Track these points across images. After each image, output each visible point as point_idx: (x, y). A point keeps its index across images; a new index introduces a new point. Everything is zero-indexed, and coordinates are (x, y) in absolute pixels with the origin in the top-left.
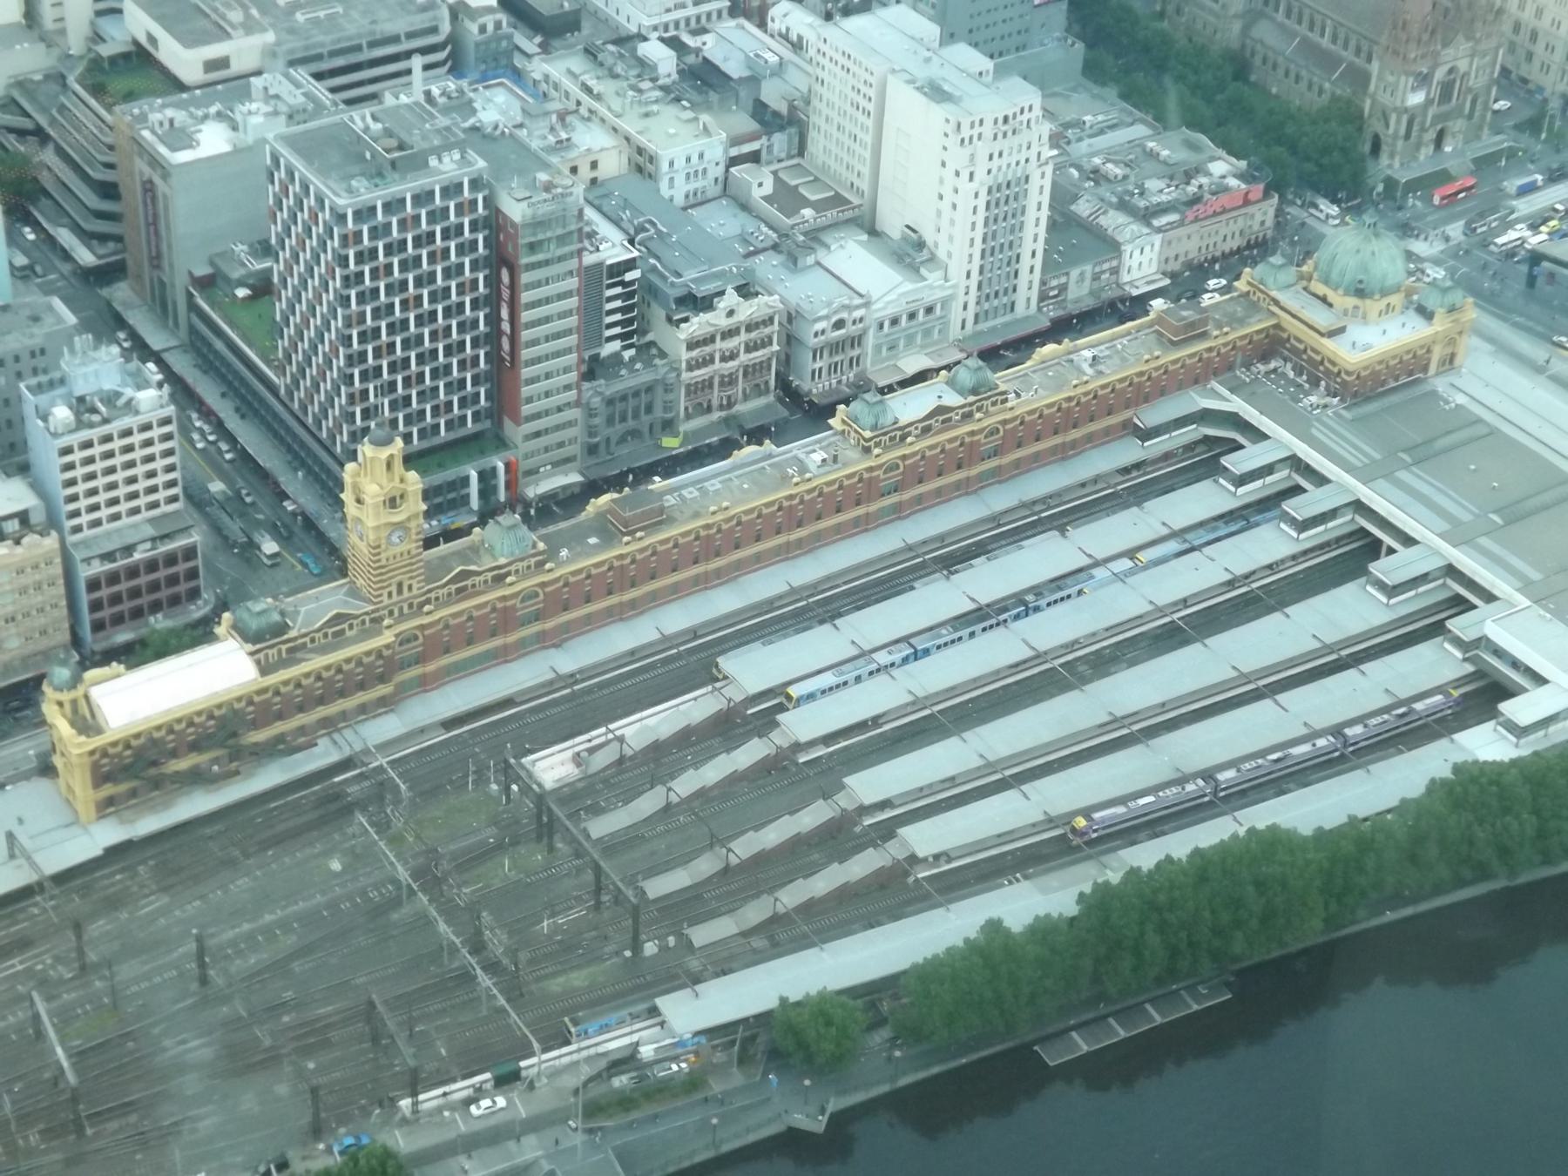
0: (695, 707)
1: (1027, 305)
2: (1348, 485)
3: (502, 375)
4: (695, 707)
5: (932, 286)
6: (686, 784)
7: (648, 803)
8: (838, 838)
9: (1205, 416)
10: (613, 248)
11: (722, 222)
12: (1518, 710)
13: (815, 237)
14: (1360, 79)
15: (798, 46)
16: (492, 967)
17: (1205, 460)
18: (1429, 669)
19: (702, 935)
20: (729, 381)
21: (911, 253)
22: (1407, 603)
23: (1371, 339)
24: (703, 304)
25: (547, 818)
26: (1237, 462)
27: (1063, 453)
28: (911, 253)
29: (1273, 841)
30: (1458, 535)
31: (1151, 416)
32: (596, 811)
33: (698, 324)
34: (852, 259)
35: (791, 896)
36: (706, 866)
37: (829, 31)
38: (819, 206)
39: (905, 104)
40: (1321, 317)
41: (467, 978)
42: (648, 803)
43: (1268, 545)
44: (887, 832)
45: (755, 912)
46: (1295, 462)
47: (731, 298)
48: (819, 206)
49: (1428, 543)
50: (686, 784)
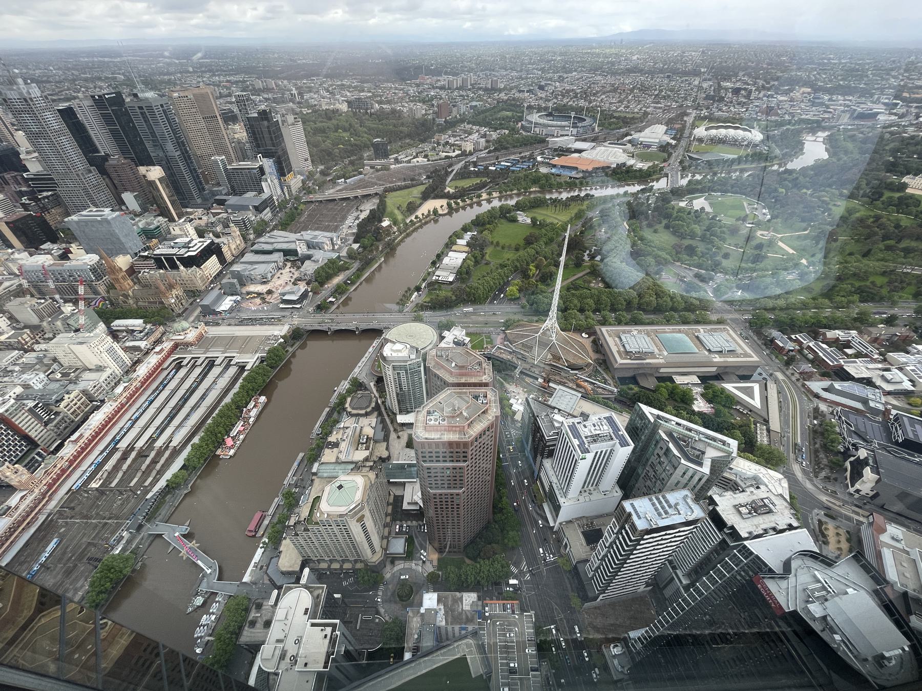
0: (117, 456)
1: (129, 362)
2: (203, 356)
3: (26, 438)
4: (117, 456)
5: (108, 372)
6: (125, 467)
7: (120, 475)
8: (160, 453)
9: (174, 360)
10: (31, 404)
11: (54, 386)
12: (248, 367)
13: (77, 378)
14: (162, 303)
15: (46, 350)
16: (109, 519)
17: (179, 367)
18: (232, 371)
19: (146, 484)
20: (79, 408)
21: (100, 369)
22: (223, 365)
23: (191, 336)
24: (62, 399)
25: (100, 491)
26: (184, 363)
27: (154, 380)
28: (100, 369)
29: (226, 405)
30: (223, 352)
31: (165, 365)
32: (111, 483)
33: (63, 404)
34: (87, 375)
35: (158, 466)
36: (139, 474)
37: (49, 345)
38: (74, 372)
39: (78, 349)
40: (182, 337)
41: (106, 523)
42: (120, 475)
43: (198, 371)
44: (167, 447)
45: (154, 473)
46: (193, 358)
47: (66, 396)
48: (74, 372)
49: (219, 355)
50: (125, 467)
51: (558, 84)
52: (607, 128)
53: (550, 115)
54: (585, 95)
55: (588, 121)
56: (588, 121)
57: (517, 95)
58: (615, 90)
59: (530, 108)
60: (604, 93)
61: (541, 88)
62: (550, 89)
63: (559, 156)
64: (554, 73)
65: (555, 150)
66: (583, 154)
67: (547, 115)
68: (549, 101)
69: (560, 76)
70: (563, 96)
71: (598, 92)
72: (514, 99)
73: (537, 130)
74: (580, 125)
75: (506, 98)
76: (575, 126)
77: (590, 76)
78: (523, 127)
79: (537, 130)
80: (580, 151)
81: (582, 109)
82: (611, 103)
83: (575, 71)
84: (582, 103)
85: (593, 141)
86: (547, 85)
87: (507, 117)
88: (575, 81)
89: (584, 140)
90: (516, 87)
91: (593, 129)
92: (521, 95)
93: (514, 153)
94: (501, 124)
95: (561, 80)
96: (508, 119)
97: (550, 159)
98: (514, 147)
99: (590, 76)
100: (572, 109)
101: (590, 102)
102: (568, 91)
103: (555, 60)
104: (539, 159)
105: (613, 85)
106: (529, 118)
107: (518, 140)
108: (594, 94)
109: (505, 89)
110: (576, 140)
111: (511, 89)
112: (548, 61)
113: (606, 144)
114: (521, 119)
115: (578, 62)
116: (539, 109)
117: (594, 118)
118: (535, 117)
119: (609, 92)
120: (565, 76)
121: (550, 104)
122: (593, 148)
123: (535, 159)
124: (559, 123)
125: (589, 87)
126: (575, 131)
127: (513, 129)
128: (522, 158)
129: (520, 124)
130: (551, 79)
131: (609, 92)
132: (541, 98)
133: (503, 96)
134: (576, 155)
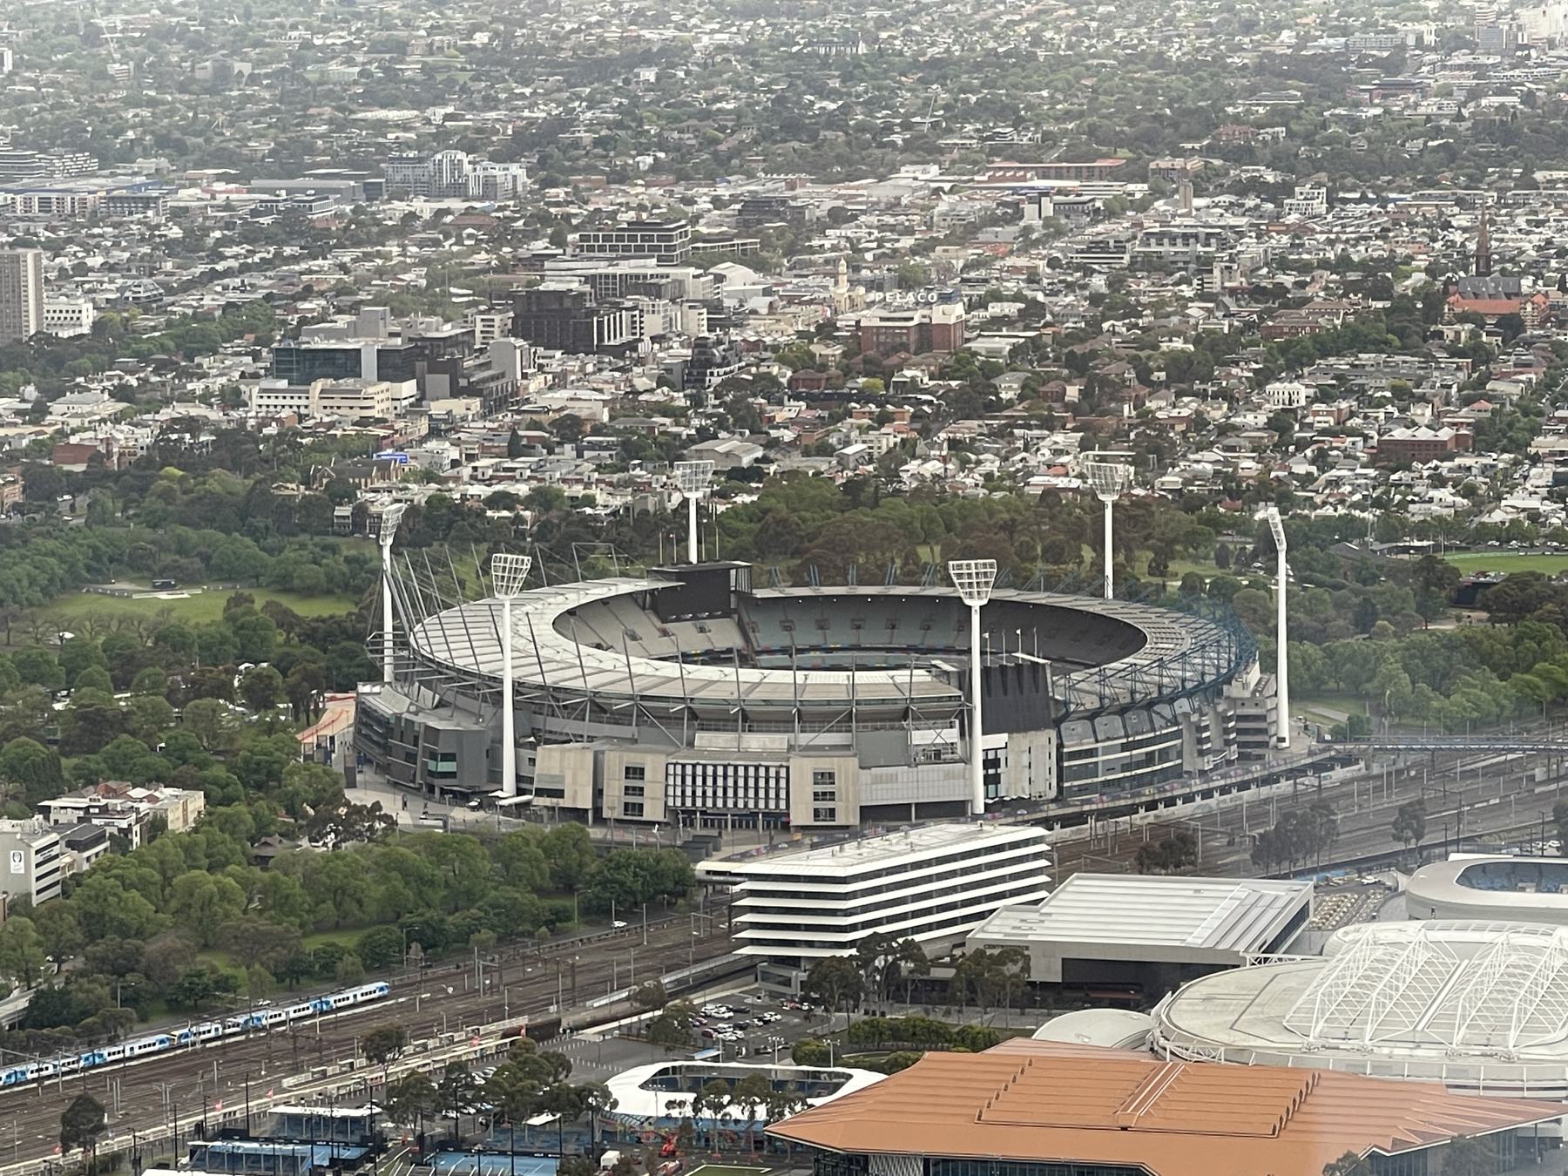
51: (739, 277)
52: (1406, 712)
53: (689, 597)
54: (1078, 375)
55: (1173, 647)
56: (1173, 647)
57: (270, 403)
58: (1409, 325)
59: (448, 536)
60: (1292, 358)
61: (556, 324)
62: (666, 329)
63: (890, 1048)
64: (679, 169)
65: (829, 983)
66: (1189, 1012)
67: (661, 606)
68: (671, 452)
69: (756, 210)
70: (829, 398)
71: (1216, 349)
72: (236, 446)
73: (568, 768)
74: (1080, 686)
75: (134, 437)
76: (1016, 701)
77: (1100, 192)
78: (379, 740)
79: (568, 768)
80: (1133, 981)
81: (1063, 525)
82: (1391, 456)
83: (923, 149)
84: (1057, 462)
85: (1275, 852)
86: (610, 291)
87: (172, 640)
88: (917, 242)
89: (1168, 854)
90: (239, 322)
91: (1252, 734)
92: (316, 403)
93: (301, 1050)
94: (93, 728)
95: (769, 235)
96: (196, 662)
97: (778, 1093)
98: (294, 976)
99: (1100, 192)
100: (954, 524)
101: (1154, 450)
102: (873, 353)
103: (670, 55)
104: (634, 1095)
105: (1374, 278)
106: (449, 639)
107: (333, 895)
108: (1183, 374)
109: (108, 342)
110: (1067, 862)
111: (193, 341)
112: (595, 68)
113: (1436, 881)
114: (345, 657)
115: (938, 69)
116: (561, 543)
117: (1246, 622)
118: (516, 634)
119: (1351, 340)
120: (816, 198)
121: (687, 488)
122: (1287, 938)
123: (582, 1104)
124: (827, 683)
125: (1114, 303)
126: (1030, 762)
127: (262, 776)
128: (408, 1096)
129: (338, 716)
130: (648, 236)
131: (1351, 340)
132: (569, 428)
133: (89, 415)
134: (1098, 1029)
